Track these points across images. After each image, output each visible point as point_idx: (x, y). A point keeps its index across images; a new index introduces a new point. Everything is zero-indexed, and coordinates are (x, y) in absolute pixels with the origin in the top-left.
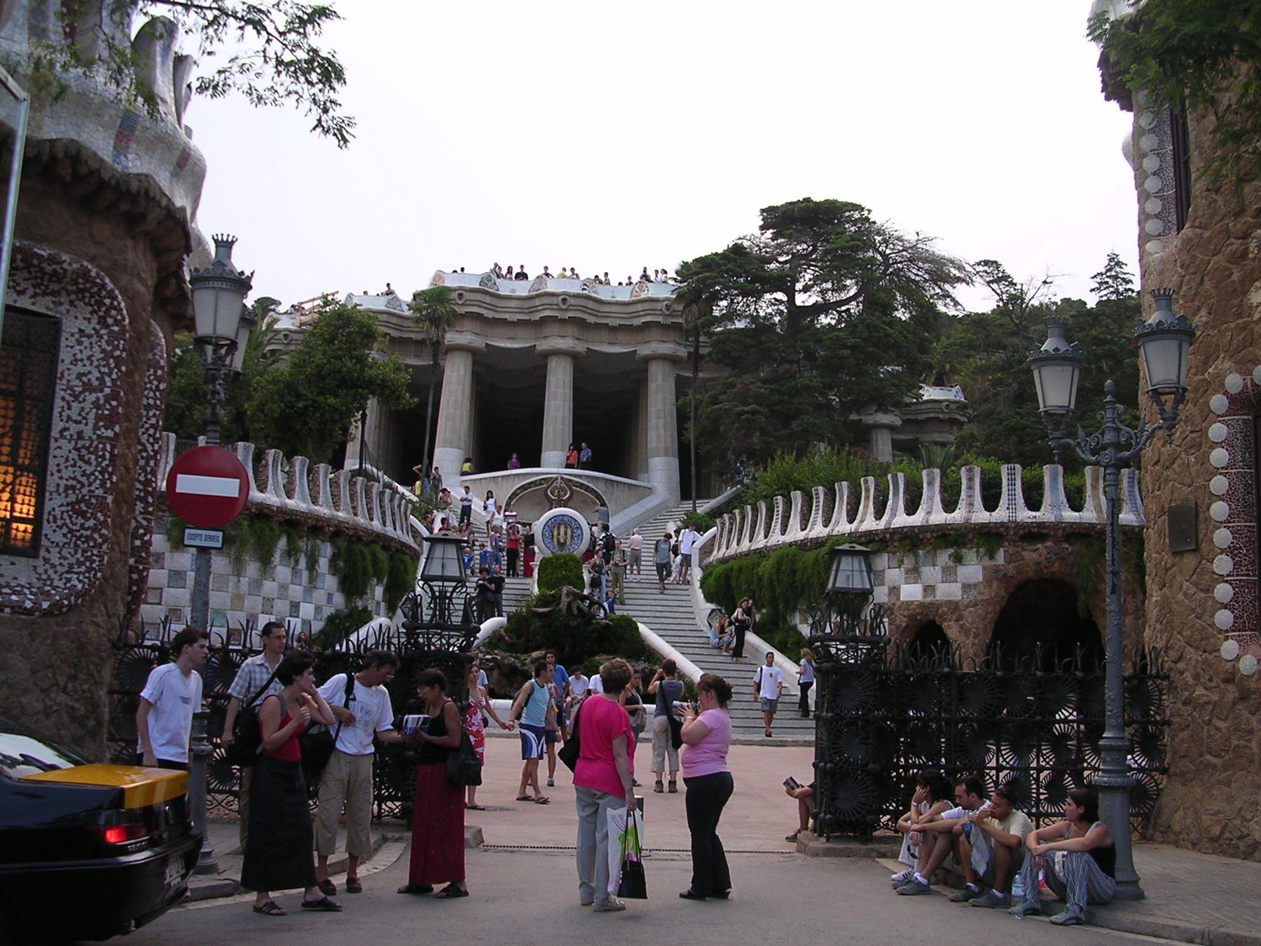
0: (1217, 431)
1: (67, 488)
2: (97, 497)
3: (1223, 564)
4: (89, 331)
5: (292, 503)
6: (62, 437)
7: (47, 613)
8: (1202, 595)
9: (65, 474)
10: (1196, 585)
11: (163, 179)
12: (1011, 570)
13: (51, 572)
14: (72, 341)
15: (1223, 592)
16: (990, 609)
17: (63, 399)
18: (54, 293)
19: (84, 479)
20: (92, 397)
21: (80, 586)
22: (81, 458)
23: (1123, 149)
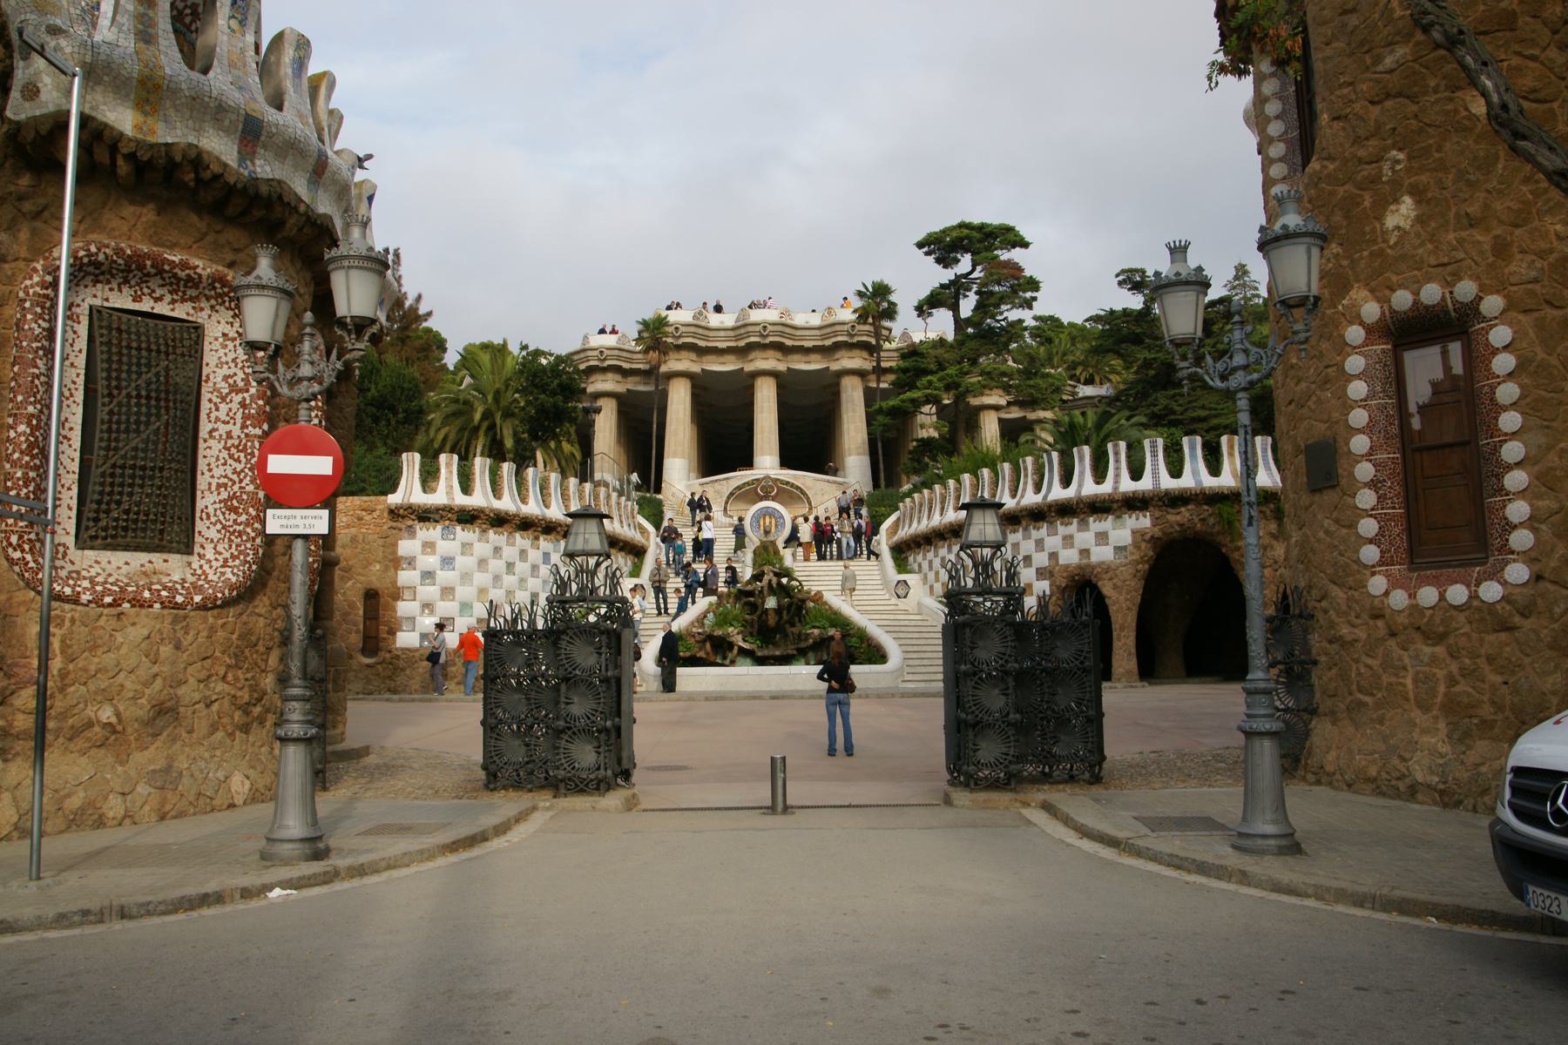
1: (219, 486)
2: (248, 493)
3: (1366, 499)
4: (232, 334)
5: (498, 505)
6: (211, 437)
7: (202, 607)
8: (1344, 531)
9: (217, 472)
10: (1337, 521)
11: (300, 186)
12: (1157, 532)
13: (206, 567)
14: (216, 345)
15: (1368, 527)
18: (192, 299)
19: (235, 477)
20: (238, 398)
21: (234, 579)
22: (231, 456)
23: (1247, 121)
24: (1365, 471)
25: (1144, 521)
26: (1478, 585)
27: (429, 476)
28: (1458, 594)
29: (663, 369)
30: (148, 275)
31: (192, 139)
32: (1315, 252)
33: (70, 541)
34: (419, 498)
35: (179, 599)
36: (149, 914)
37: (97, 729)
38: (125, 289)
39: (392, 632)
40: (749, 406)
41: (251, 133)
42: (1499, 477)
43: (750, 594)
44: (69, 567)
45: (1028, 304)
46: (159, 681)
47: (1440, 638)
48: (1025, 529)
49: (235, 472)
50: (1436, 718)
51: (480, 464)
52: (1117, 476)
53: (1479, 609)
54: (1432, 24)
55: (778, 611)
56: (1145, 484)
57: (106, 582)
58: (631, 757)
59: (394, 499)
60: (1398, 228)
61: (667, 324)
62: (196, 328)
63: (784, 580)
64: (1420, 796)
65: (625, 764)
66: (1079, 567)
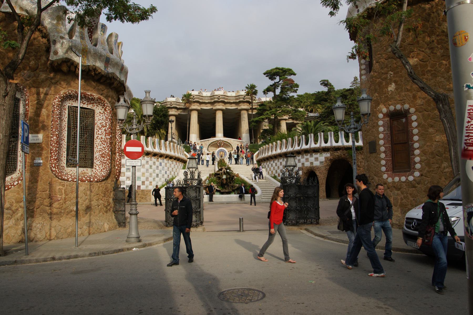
1: (99, 151)
3: (383, 156)
4: (102, 112)
7: (97, 182)
9: (99, 147)
10: (376, 161)
11: (118, 74)
14: (98, 115)
15: (383, 162)
18: (92, 103)
20: (104, 129)
22: (102, 143)
24: (383, 149)
25: (328, 155)
28: (403, 179)
31: (94, 64)
32: (370, 103)
33: (65, 165)
36: (108, 253)
37: (73, 212)
42: (413, 151)
43: (219, 174)
44: (65, 172)
45: (295, 91)
46: (87, 200)
47: (398, 189)
49: (103, 147)
50: (398, 208)
52: (321, 142)
53: (408, 182)
54: (396, 53)
55: (226, 179)
58: (203, 219)
60: (391, 91)
61: (191, 95)
63: (228, 171)
65: (202, 220)
66: (310, 167)
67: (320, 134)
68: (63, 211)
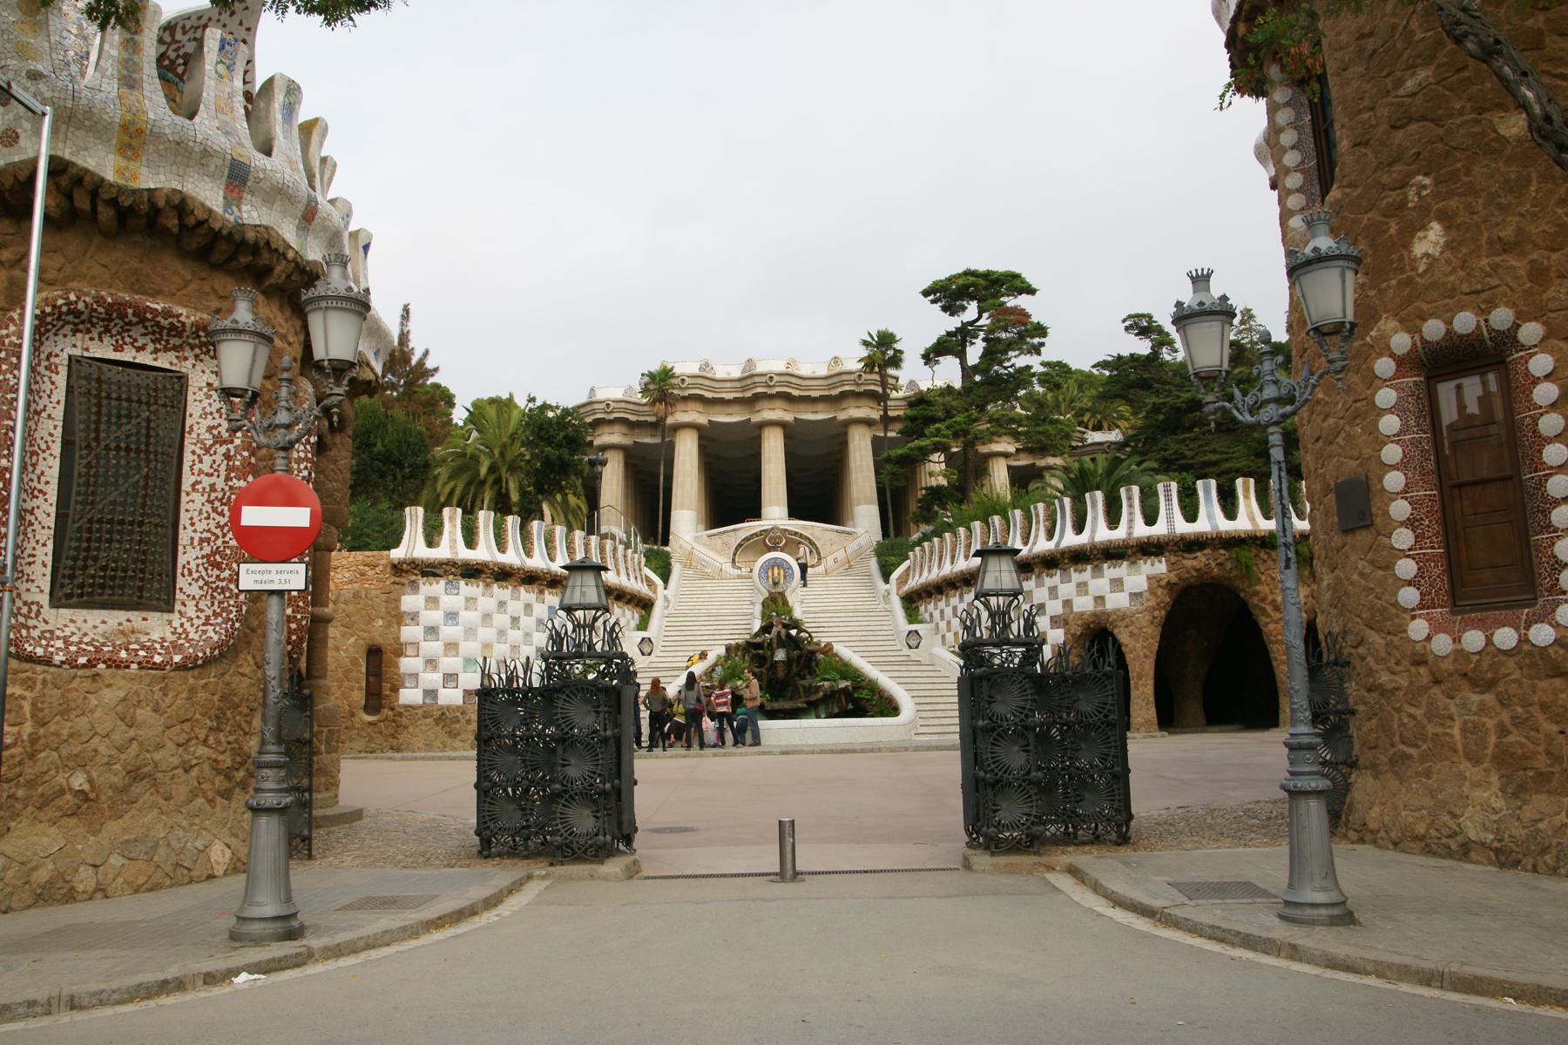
0: (1386, 397)
1: (202, 540)
2: (231, 548)
3: (1403, 538)
5: (502, 558)
6: (194, 490)
7: (181, 667)
8: (1381, 573)
9: (200, 526)
10: (1372, 563)
11: (288, 232)
12: (1173, 578)
13: (187, 625)
15: (1406, 568)
16: (1157, 613)
17: (193, 452)
18: (175, 348)
19: (218, 531)
20: (223, 450)
22: (215, 510)
23: (1259, 155)
24: (1400, 509)
25: (1160, 567)
26: (1527, 628)
27: (432, 534)
28: (1506, 637)
29: (670, 420)
30: (130, 323)
31: (176, 185)
32: (1349, 275)
33: (44, 599)
34: (422, 552)
35: (158, 659)
36: (102, 1003)
37: (68, 797)
38: (106, 339)
39: (395, 690)
40: (756, 457)
41: (238, 178)
42: (1546, 513)
43: (758, 646)
45: (1036, 350)
46: (135, 746)
47: (1488, 686)
48: (1039, 576)
49: (218, 526)
50: (1487, 770)
51: (485, 518)
52: (1131, 521)
53: (1530, 654)
54: (1466, 35)
55: (789, 662)
56: (1160, 529)
57: (80, 642)
59: (397, 554)
60: (1427, 255)
61: (673, 376)
62: (180, 378)
63: (793, 632)
64: (1473, 855)
66: (1094, 614)
67: (1129, 491)
68: (21, 793)
